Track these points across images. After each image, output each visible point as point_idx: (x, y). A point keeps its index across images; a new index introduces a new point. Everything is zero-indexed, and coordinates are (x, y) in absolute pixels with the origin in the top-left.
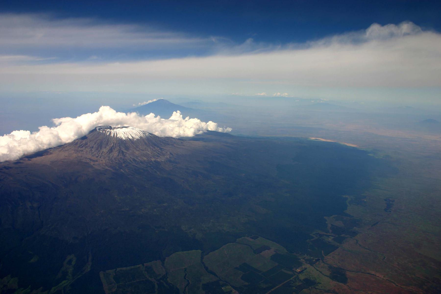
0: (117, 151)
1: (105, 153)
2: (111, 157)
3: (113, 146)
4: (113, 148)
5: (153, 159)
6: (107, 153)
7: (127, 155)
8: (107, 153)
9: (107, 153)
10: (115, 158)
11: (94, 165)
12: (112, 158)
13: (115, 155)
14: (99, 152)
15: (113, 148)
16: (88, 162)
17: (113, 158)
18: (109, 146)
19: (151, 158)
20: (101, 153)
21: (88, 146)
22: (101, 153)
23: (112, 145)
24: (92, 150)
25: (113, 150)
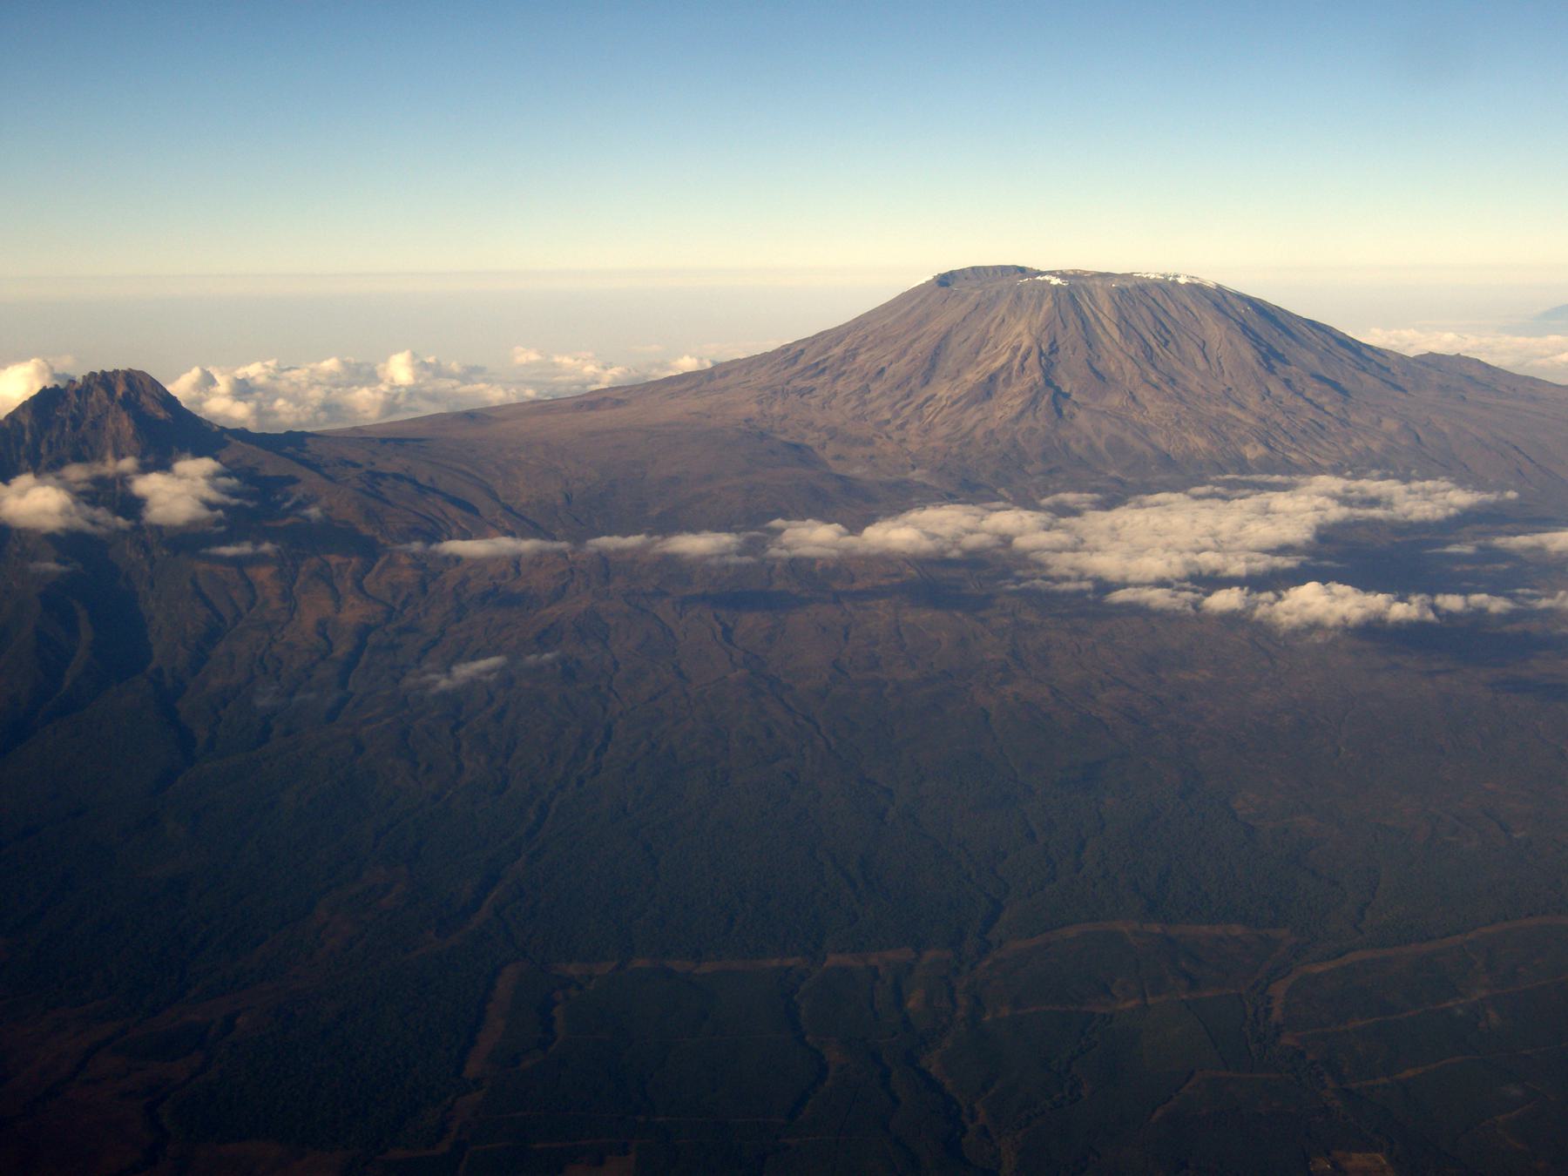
0: (1022, 393)
1: (944, 402)
2: (969, 424)
3: (1006, 367)
4: (1003, 376)
5: (1255, 447)
6: (950, 407)
7: (1082, 418)
8: (954, 403)
9: (954, 403)
10: (992, 432)
11: (838, 457)
12: (975, 426)
13: (999, 414)
14: (908, 401)
15: (1003, 376)
16: (809, 443)
17: (979, 432)
18: (978, 365)
19: (1245, 443)
20: (914, 405)
21: (852, 371)
22: (914, 405)
23: (1002, 360)
24: (867, 389)
25: (1000, 387)
